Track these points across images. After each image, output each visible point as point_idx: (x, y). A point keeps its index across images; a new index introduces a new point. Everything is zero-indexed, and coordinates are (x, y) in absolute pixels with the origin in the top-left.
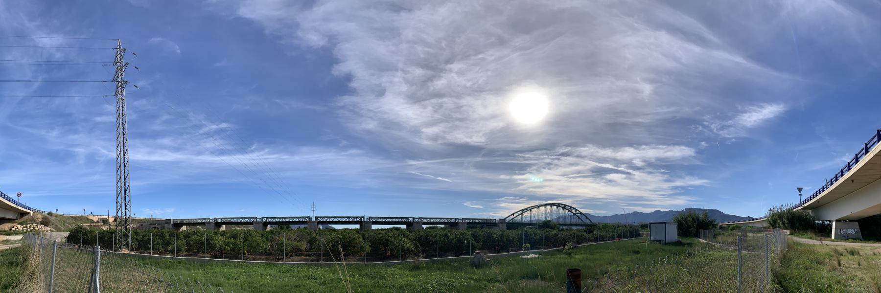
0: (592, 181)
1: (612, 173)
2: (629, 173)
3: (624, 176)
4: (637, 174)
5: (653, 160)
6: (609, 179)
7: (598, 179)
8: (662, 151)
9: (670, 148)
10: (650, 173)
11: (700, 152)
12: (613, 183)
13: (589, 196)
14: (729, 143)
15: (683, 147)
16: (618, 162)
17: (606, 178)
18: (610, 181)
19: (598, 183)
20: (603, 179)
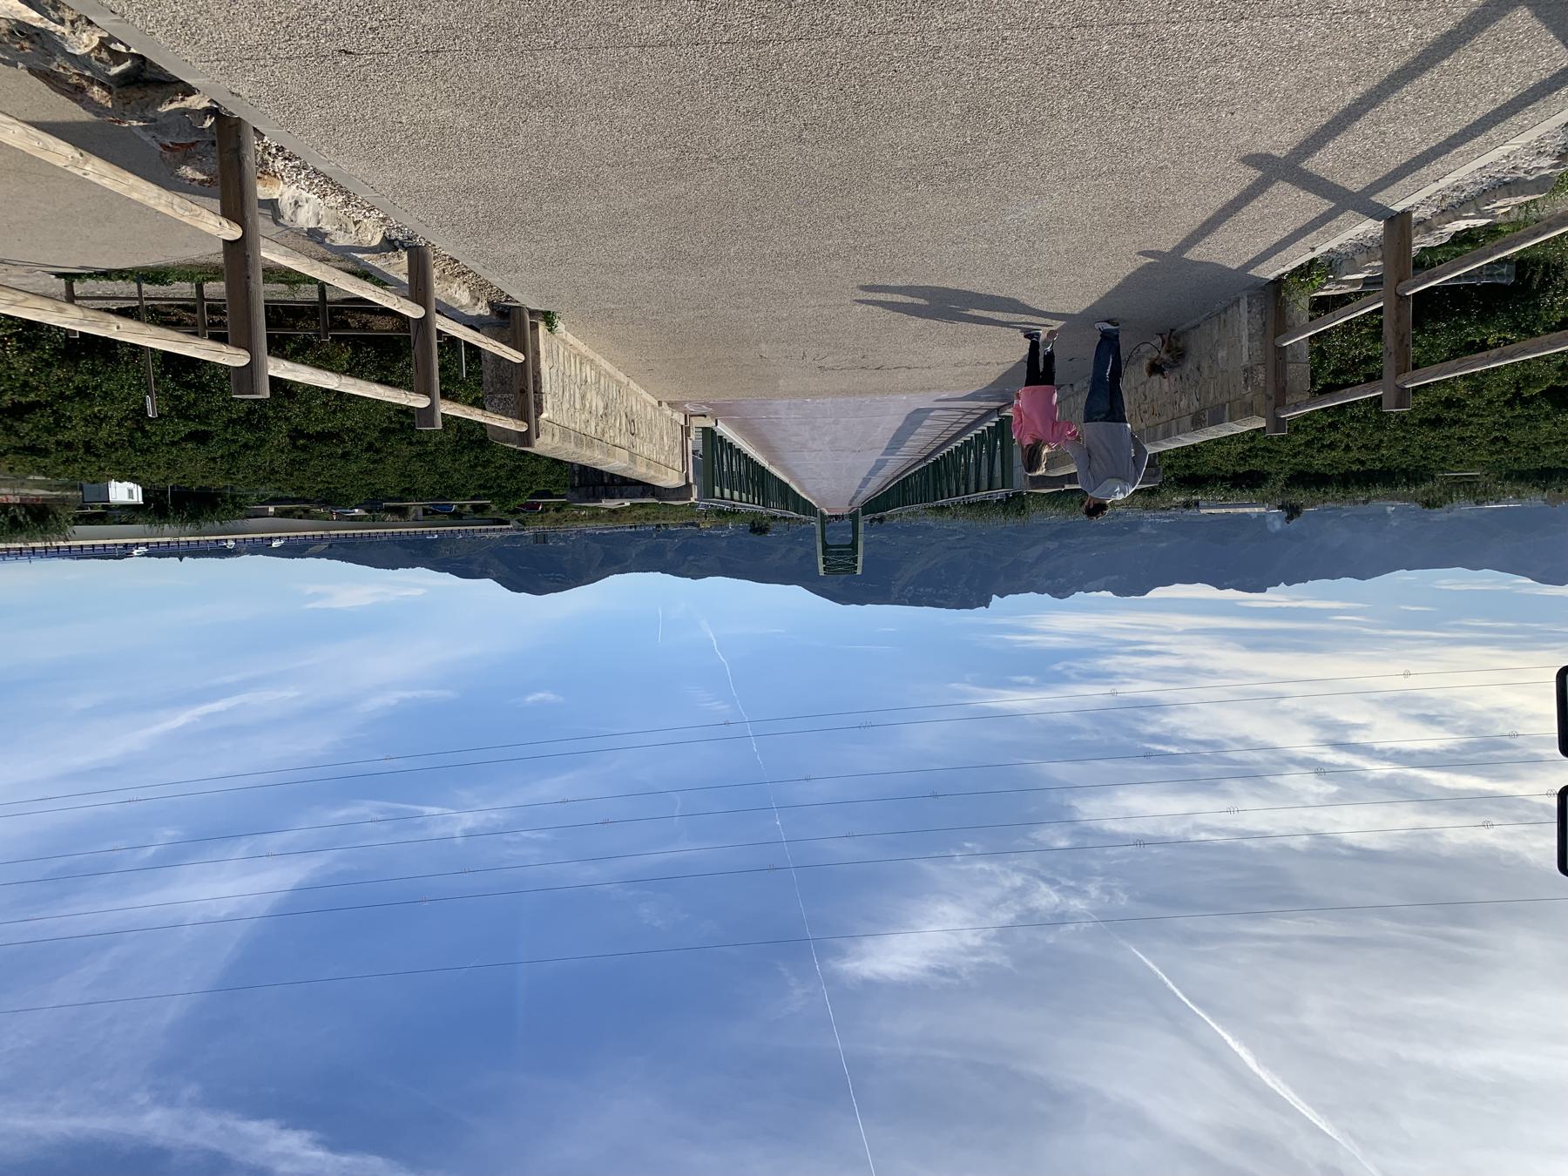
0: (1533, 724)
1: (1424, 752)
2: (1339, 746)
3: (1356, 738)
4: (1302, 742)
5: (1234, 785)
6: (1441, 729)
7: (1502, 729)
8: (1201, 820)
9: (1173, 831)
10: (1242, 740)
11: (1062, 816)
12: (1414, 712)
13: (1538, 653)
14: (967, 845)
15: (1120, 827)
16: (1395, 790)
17: (1457, 733)
18: (1430, 720)
19: (1500, 710)
20: (1471, 731)
